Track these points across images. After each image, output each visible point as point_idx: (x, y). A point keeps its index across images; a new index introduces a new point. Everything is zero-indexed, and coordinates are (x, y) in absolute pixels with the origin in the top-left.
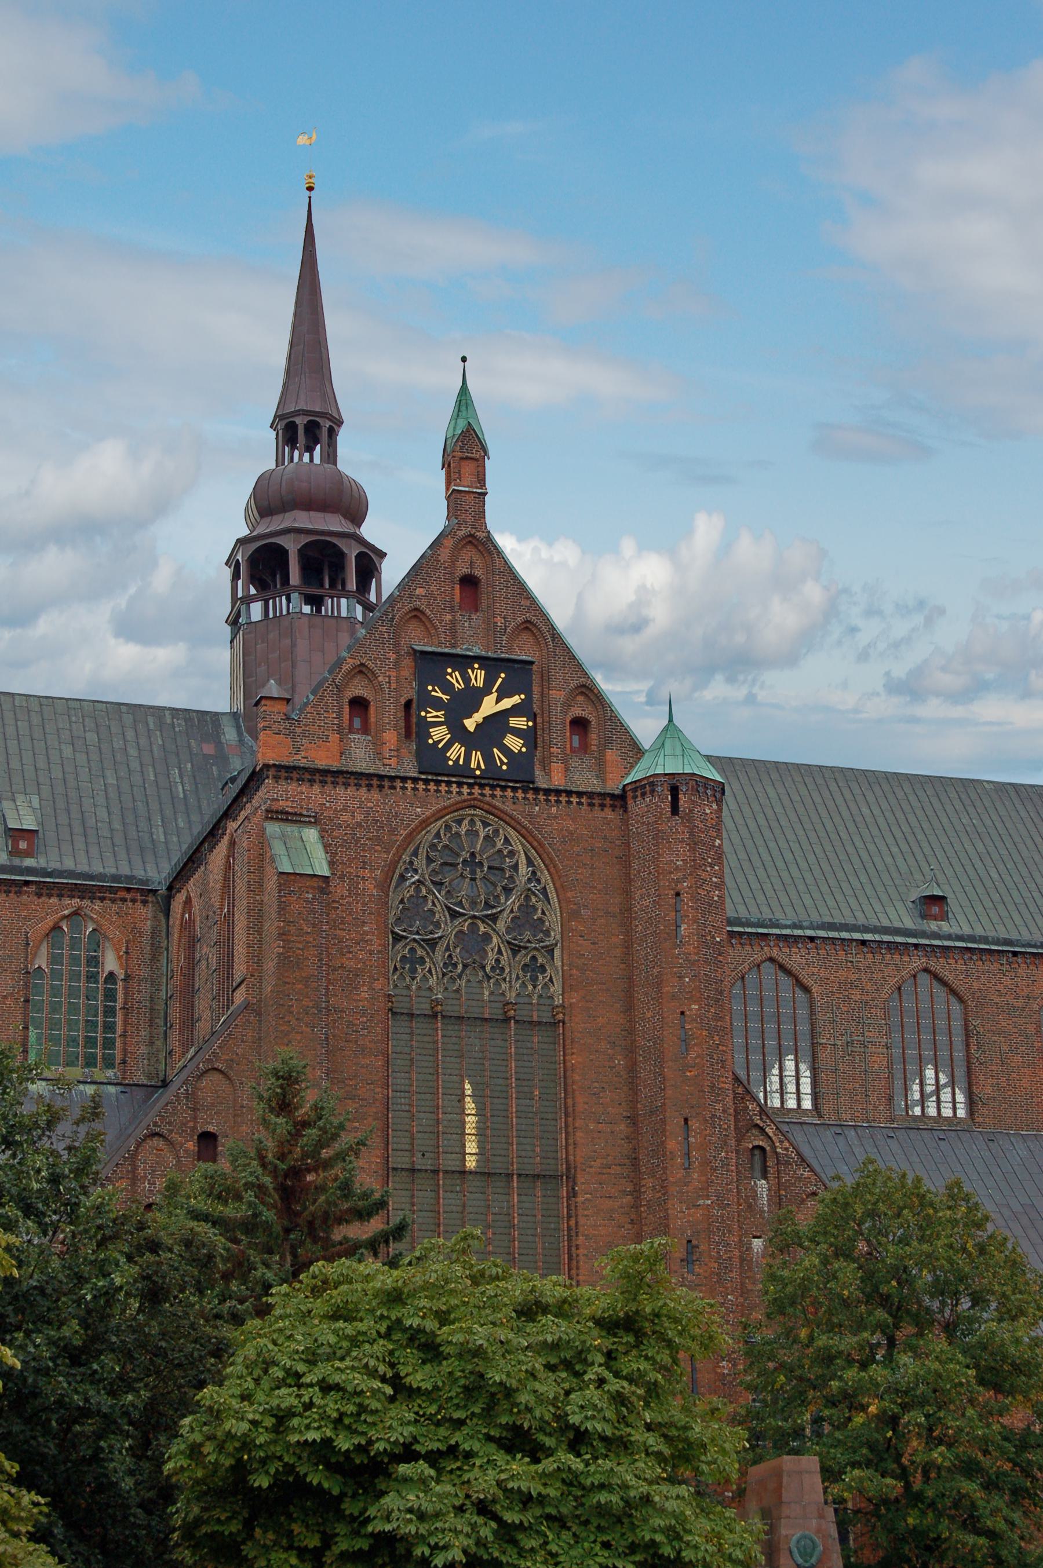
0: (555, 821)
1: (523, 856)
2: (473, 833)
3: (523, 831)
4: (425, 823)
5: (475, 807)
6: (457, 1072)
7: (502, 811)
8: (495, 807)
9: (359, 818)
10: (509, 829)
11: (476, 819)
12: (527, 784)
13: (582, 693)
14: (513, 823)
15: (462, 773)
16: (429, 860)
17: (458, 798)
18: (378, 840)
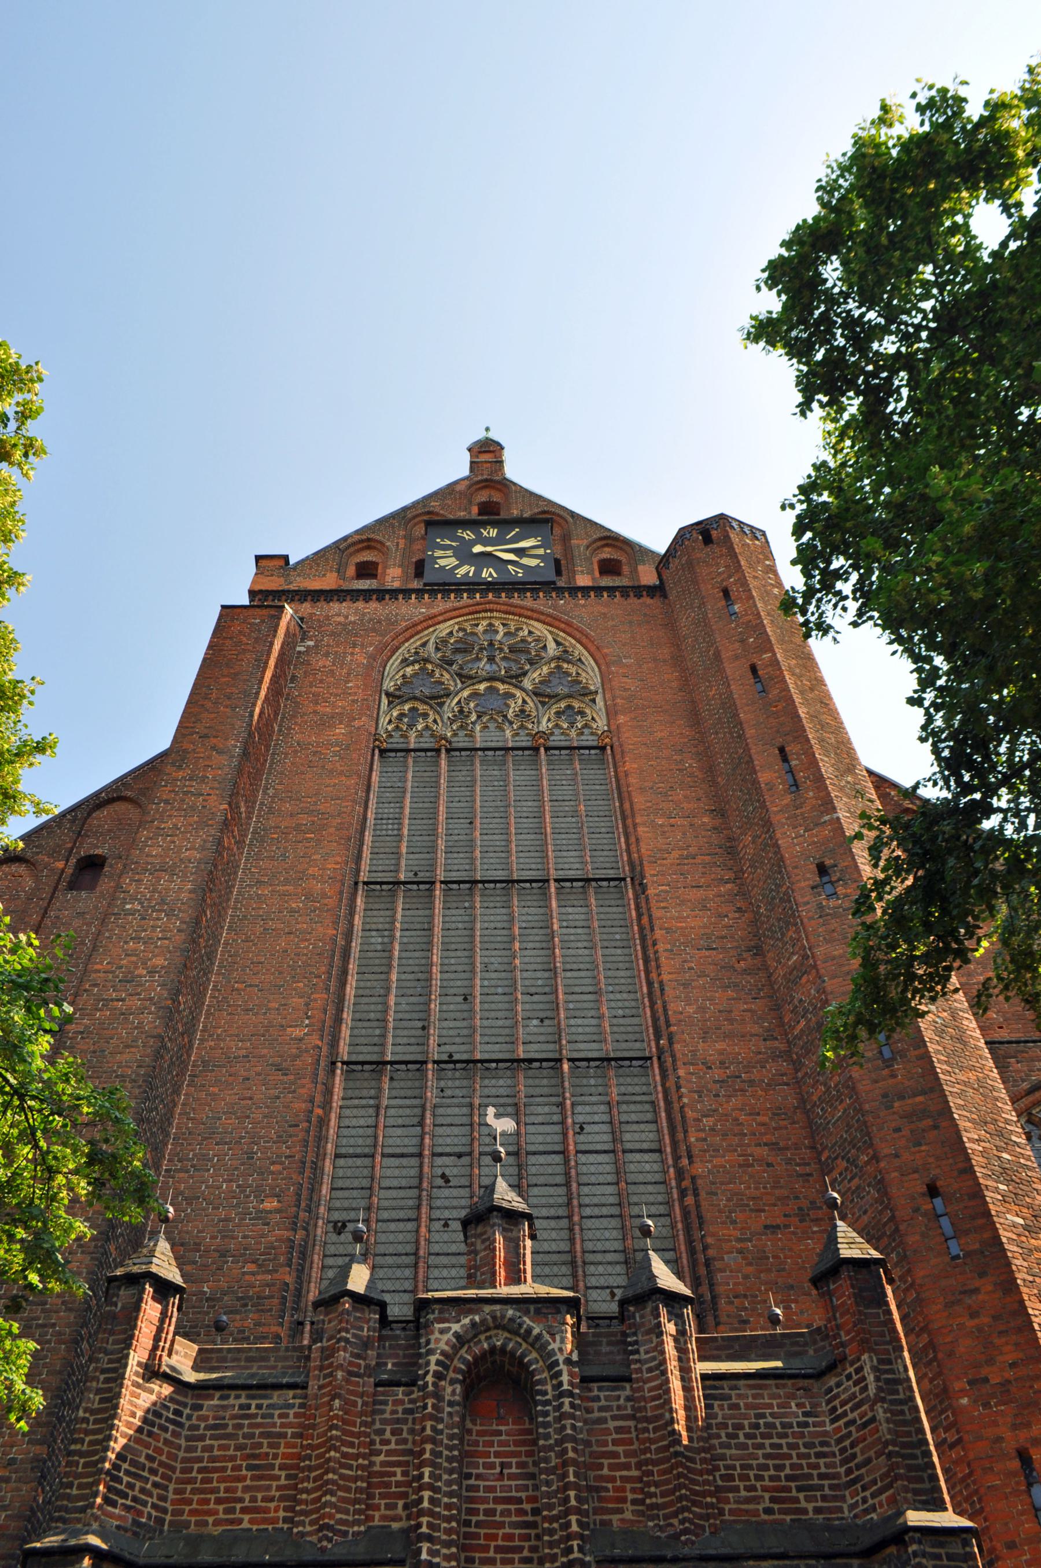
0: (583, 611)
1: (550, 637)
2: (491, 629)
3: (548, 620)
4: (432, 621)
5: (491, 611)
6: (593, 1013)
7: (522, 608)
8: (511, 605)
9: (352, 618)
10: (532, 622)
11: (493, 621)
12: (548, 587)
13: (607, 545)
14: (535, 615)
15: (472, 586)
16: (437, 649)
17: (471, 601)
18: (374, 630)
